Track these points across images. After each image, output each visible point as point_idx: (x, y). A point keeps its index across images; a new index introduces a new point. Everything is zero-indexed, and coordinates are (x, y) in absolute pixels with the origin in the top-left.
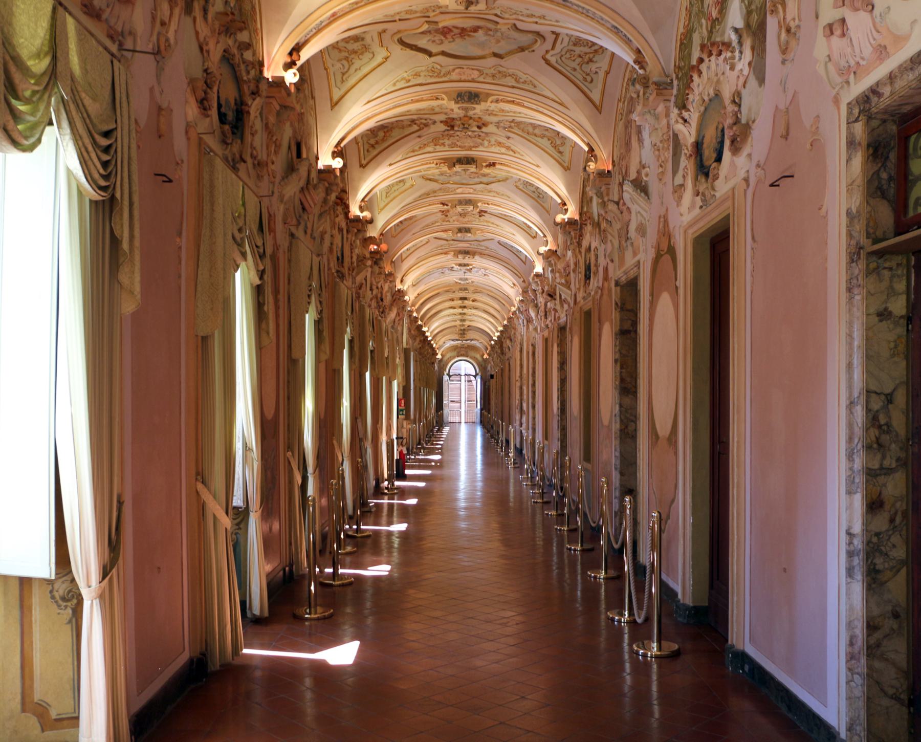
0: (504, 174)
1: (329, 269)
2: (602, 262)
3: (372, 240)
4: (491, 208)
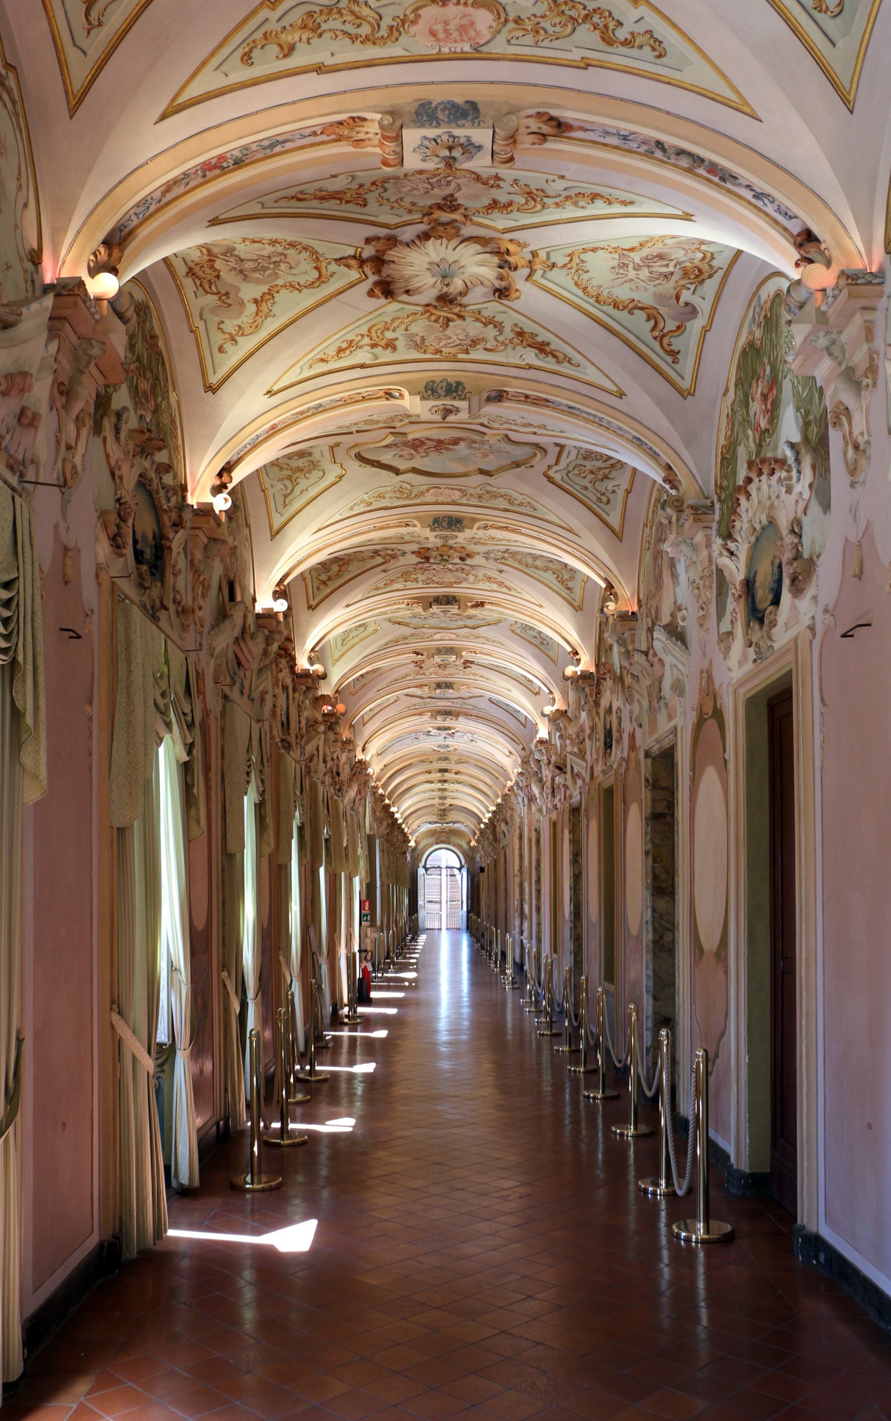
0: (495, 616)
2: (627, 727)
3: (324, 699)
4: (479, 658)
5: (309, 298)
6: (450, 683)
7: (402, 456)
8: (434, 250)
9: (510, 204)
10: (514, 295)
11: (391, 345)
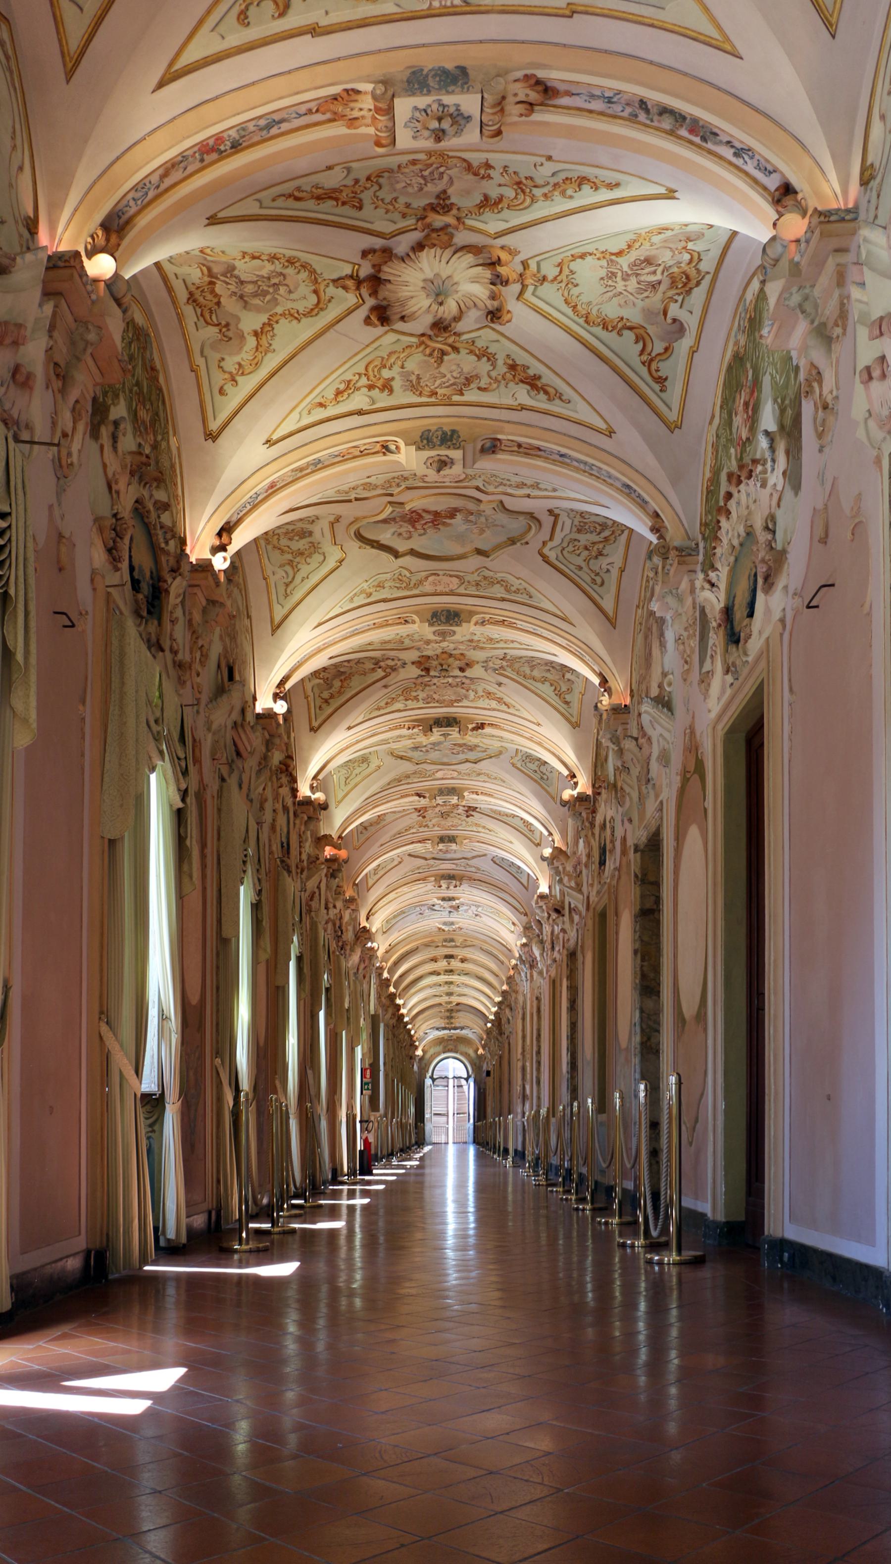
0: (496, 744)
1: (271, 853)
3: (326, 840)
4: (481, 801)
5: (307, 329)
6: (453, 836)
7: (400, 534)
8: (430, 264)
9: (500, 199)
10: (506, 317)
11: (387, 387)
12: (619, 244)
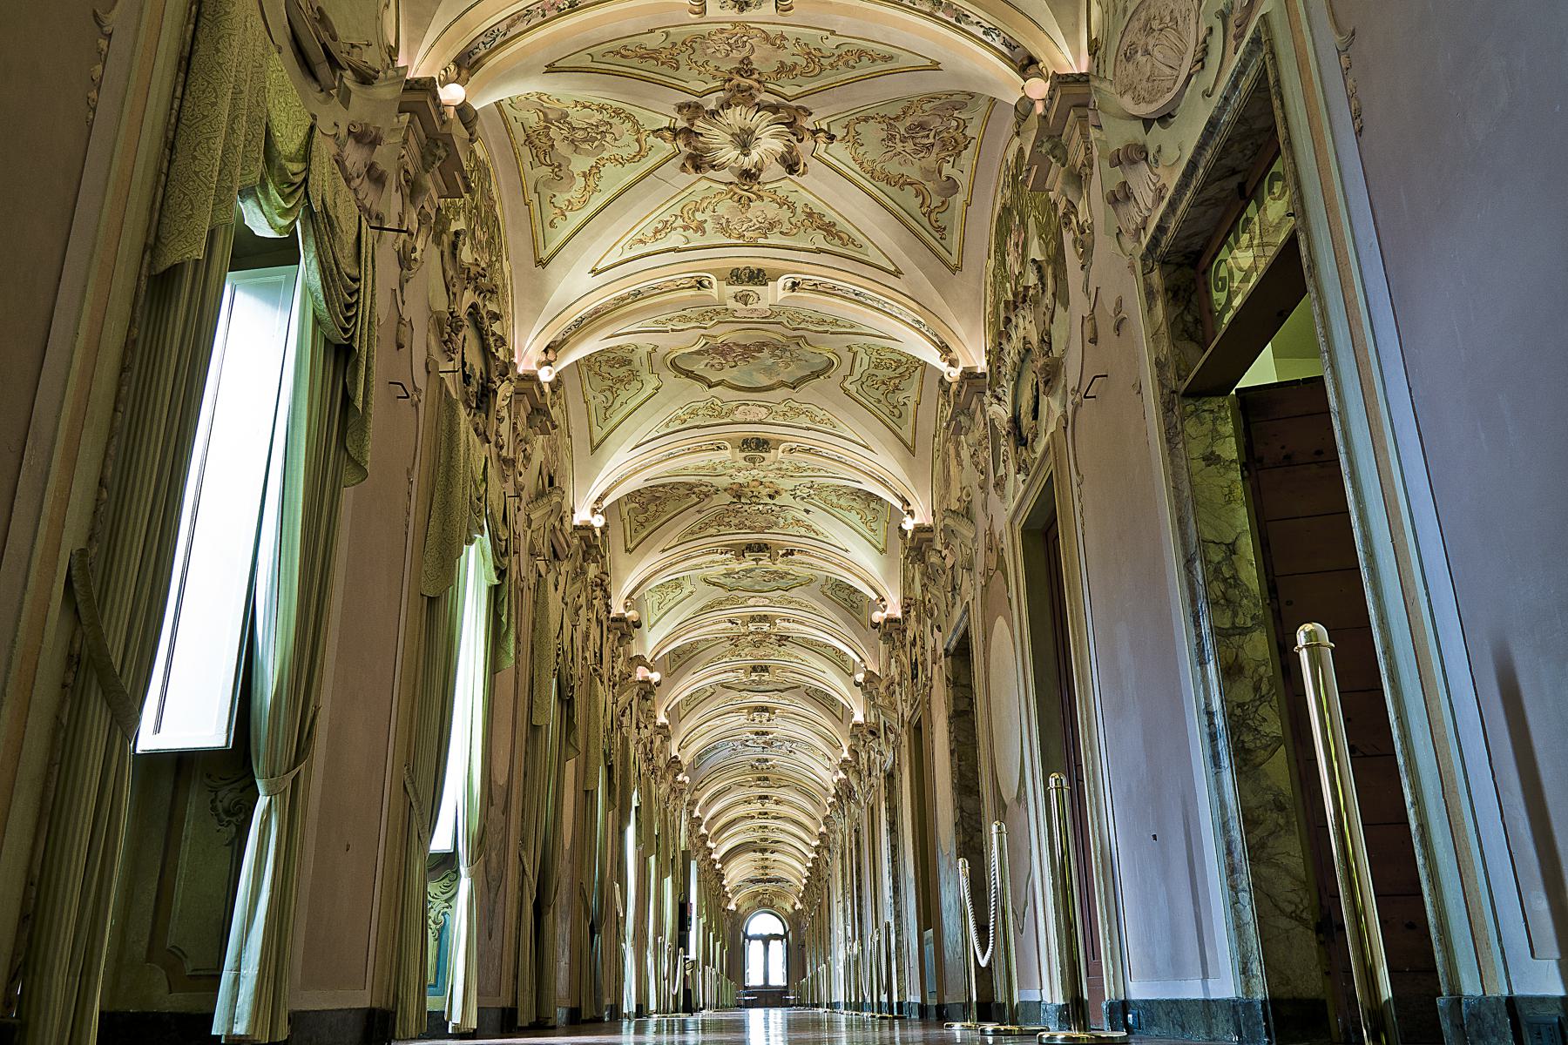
3: (640, 660)
11: (700, 228)
12: (896, 110)
